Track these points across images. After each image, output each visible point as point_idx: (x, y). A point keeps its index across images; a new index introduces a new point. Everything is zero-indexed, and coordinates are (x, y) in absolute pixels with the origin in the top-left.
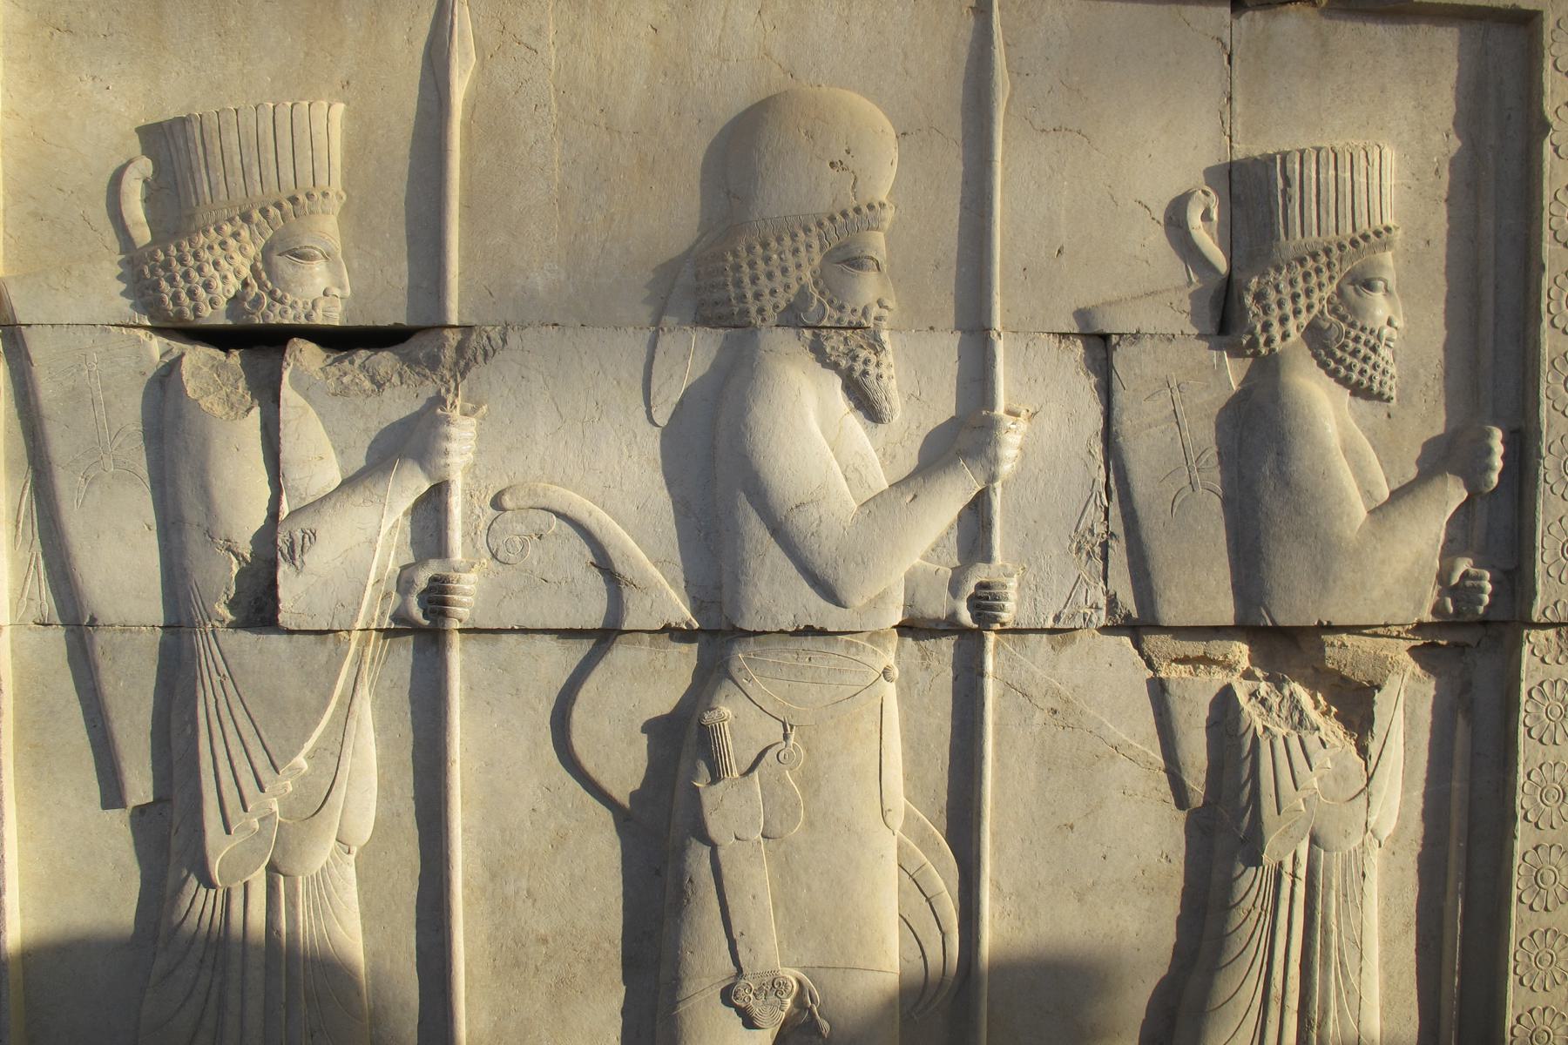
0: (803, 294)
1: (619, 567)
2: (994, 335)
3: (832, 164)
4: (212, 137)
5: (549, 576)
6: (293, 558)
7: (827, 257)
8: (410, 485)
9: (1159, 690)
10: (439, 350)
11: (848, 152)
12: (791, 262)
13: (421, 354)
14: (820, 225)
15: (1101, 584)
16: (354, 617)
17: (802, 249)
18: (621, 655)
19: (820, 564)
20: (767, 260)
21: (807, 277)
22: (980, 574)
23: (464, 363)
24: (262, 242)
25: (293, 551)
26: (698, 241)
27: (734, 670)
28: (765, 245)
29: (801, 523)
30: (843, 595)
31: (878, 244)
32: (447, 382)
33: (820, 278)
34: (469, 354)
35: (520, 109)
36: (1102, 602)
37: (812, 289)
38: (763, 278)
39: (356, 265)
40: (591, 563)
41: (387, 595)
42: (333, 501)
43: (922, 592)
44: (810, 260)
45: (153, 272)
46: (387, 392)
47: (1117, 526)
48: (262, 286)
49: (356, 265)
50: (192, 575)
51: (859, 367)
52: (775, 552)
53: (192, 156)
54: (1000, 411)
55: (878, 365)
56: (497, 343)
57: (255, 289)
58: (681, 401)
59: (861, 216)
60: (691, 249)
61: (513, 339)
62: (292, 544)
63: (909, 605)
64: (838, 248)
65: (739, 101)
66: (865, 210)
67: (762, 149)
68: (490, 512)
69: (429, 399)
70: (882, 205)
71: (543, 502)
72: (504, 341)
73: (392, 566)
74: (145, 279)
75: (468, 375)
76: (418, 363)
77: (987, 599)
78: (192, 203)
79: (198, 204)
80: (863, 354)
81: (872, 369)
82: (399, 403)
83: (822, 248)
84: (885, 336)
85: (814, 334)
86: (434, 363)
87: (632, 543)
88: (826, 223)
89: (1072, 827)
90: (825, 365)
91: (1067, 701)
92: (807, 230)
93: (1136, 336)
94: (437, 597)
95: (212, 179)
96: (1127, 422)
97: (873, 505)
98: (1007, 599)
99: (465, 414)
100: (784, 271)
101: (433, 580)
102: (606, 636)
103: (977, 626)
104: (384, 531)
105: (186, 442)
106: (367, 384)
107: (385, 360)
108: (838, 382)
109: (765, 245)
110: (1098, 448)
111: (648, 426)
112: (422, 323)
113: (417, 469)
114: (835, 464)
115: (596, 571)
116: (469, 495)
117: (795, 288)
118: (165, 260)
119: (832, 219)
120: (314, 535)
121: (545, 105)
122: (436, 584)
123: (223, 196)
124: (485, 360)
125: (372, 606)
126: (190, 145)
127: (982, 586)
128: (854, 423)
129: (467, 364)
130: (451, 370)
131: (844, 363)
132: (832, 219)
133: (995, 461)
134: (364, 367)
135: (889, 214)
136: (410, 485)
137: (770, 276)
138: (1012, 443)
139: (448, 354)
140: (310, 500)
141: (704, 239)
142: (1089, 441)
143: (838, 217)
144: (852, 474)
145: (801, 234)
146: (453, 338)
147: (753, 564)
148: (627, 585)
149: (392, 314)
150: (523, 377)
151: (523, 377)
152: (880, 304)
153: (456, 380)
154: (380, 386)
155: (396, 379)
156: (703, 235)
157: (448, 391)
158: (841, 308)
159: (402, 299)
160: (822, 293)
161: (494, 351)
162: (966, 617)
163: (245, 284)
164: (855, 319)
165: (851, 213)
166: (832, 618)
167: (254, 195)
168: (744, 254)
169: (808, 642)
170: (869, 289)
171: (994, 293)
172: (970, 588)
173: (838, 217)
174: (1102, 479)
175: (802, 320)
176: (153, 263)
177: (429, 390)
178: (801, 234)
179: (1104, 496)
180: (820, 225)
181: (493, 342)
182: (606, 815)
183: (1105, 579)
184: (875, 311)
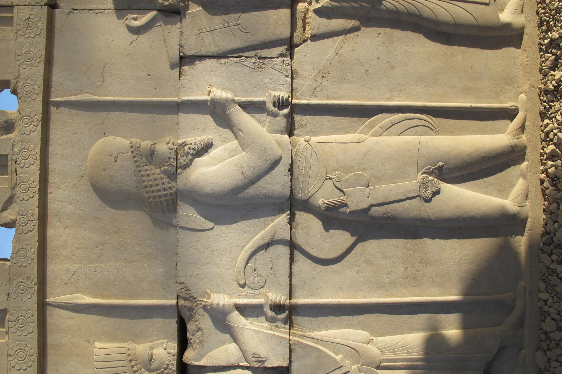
0: (164, 172)
1: (267, 241)
2: (180, 100)
3: (116, 161)
5: (270, 266)
7: (150, 163)
8: (236, 318)
9: (315, 38)
11: (111, 155)
12: (152, 177)
13: (188, 313)
14: (138, 166)
15: (274, 59)
16: (285, 339)
17: (147, 173)
18: (300, 240)
19: (265, 166)
20: (151, 186)
21: (158, 171)
22: (270, 106)
23: (191, 298)
26: (145, 211)
27: (305, 198)
28: (146, 187)
29: (250, 173)
30: (277, 158)
31: (146, 144)
32: (198, 304)
33: (158, 166)
34: (188, 296)
35: (96, 277)
36: (281, 59)
37: (162, 169)
38: (159, 187)
39: (155, 338)
40: (265, 251)
41: (277, 326)
43: (277, 128)
44: (152, 170)
46: (202, 326)
47: (252, 53)
49: (155, 338)
51: (191, 152)
52: (261, 183)
54: (208, 98)
55: (191, 144)
56: (183, 286)
58: (205, 218)
59: (135, 151)
60: (148, 214)
61: (182, 280)
63: (281, 132)
64: (147, 159)
65: (93, 196)
66: (133, 149)
67: (110, 188)
68: (246, 288)
69: (204, 311)
70: (131, 143)
71: (242, 269)
72: (183, 283)
73: (266, 324)
75: (195, 297)
76: (191, 315)
77: (279, 103)
80: (187, 150)
81: (192, 147)
82: (206, 322)
83: (147, 165)
84: (180, 142)
85: (179, 168)
86: (191, 309)
87: (258, 236)
88: (137, 164)
89: (367, 71)
90: (191, 164)
91: (319, 72)
92: (140, 171)
93: (181, 46)
94: (278, 308)
96: (213, 50)
97: (243, 146)
98: (279, 96)
99: (210, 298)
100: (155, 179)
101: (271, 309)
102: (292, 246)
103: (290, 107)
104: (253, 328)
106: (199, 333)
107: (190, 327)
108: (197, 159)
109: (146, 187)
110: (223, 61)
111: (214, 230)
112: (176, 313)
113: (230, 315)
114: (228, 160)
115: (268, 249)
116: (240, 296)
117: (162, 175)
119: (136, 161)
121: (95, 268)
122: (272, 308)
124: (190, 290)
125: (281, 332)
127: (274, 105)
128: (213, 153)
129: (191, 297)
130: (193, 303)
131: (190, 157)
132: (136, 161)
133: (227, 100)
134: (193, 334)
135: (135, 140)
136: (236, 318)
137: (157, 185)
138: (220, 94)
139: (188, 304)
141: (144, 209)
142: (220, 64)
143: (135, 159)
144: (232, 154)
145: (142, 173)
146: (182, 302)
147: (265, 191)
148: (273, 238)
149: (173, 325)
150: (196, 276)
151: (196, 276)
152: (168, 143)
153: (197, 301)
154: (199, 329)
155: (197, 323)
157: (201, 304)
158: (169, 158)
159: (167, 321)
160: (164, 165)
161: (186, 287)
162: (286, 111)
164: (174, 153)
165: (134, 154)
166: (286, 161)
168: (149, 195)
169: (295, 170)
170: (163, 148)
171: (164, 100)
172: (275, 110)
173: (135, 159)
174: (235, 59)
177: (201, 311)
178: (142, 173)
179: (241, 58)
180: (138, 166)
181: (183, 287)
182: (360, 245)
183: (272, 58)
184: (171, 145)
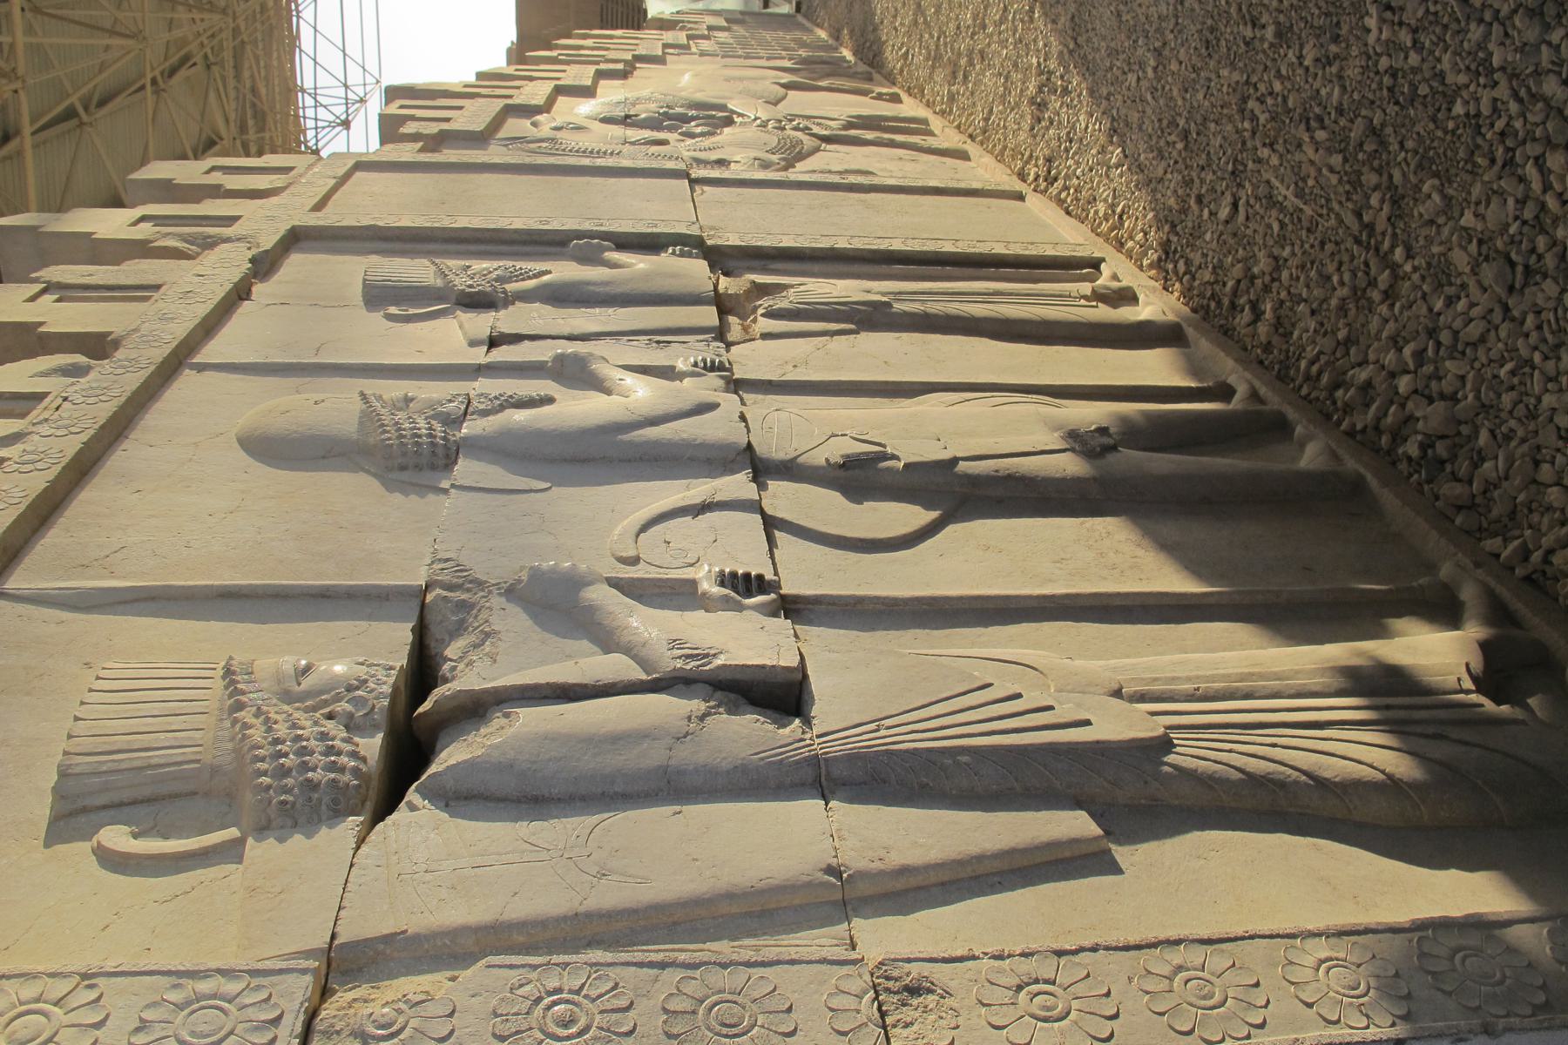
4: (105, 743)
6: (706, 656)
10: (451, 601)
24: (275, 701)
25: (698, 655)
26: (368, 472)
27: (789, 457)
34: (460, 581)
42: (631, 638)
45: (288, 791)
48: (338, 698)
50: (744, 759)
53: (124, 766)
57: (344, 706)
60: (375, 475)
62: (688, 656)
68: (642, 565)
74: (294, 804)
76: (463, 621)
78: (192, 769)
79: (198, 761)
85: (472, 414)
86: (465, 606)
95: (167, 744)
101: (722, 584)
105: (550, 760)
111: (550, 492)
112: (417, 613)
118: (272, 777)
120: (675, 641)
122: (726, 582)
123: (198, 735)
124: (466, 571)
126: (104, 768)
129: (471, 582)
130: (475, 594)
147: (685, 436)
156: (363, 470)
161: (458, 565)
163: (330, 717)
167: (207, 707)
175: (458, 418)
176: (271, 792)
182: (952, 530)
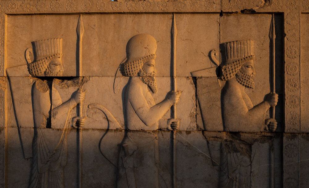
0: (140, 71)
1: (109, 118)
2: (174, 77)
3: (145, 48)
5: (97, 120)
7: (144, 64)
8: (73, 104)
11: (148, 45)
12: (138, 66)
14: (143, 58)
15: (195, 123)
17: (140, 63)
18: (109, 134)
19: (143, 118)
20: (134, 65)
21: (141, 68)
22: (172, 120)
23: (83, 82)
24: (49, 63)
28: (133, 62)
29: (140, 111)
30: (147, 124)
31: (153, 62)
32: (80, 86)
33: (143, 68)
34: (83, 81)
36: (196, 126)
37: (142, 70)
38: (133, 68)
41: (70, 123)
43: (162, 124)
44: (141, 65)
46: (70, 88)
47: (199, 112)
51: (150, 83)
52: (136, 116)
54: (176, 91)
55: (153, 83)
57: (48, 70)
59: (150, 57)
61: (91, 79)
63: (159, 126)
64: (146, 63)
66: (151, 56)
70: (154, 55)
72: (89, 79)
73: (71, 117)
75: (83, 85)
77: (173, 125)
80: (151, 81)
81: (152, 84)
82: (72, 90)
83: (143, 63)
84: (154, 78)
87: (111, 114)
88: (144, 58)
89: (191, 168)
90: (144, 82)
91: (189, 144)
92: (141, 60)
93: (201, 77)
94: (78, 123)
96: (199, 93)
97: (152, 108)
98: (177, 125)
99: (83, 92)
100: (137, 67)
102: (108, 130)
104: (69, 112)
106: (66, 86)
107: (70, 82)
108: (147, 86)
109: (133, 62)
110: (194, 98)
113: (75, 101)
114: (146, 101)
116: (83, 105)
117: (139, 70)
119: (145, 57)
125: (67, 124)
127: (172, 123)
128: (149, 93)
131: (147, 83)
132: (145, 57)
133: (175, 100)
135: (155, 56)
136: (73, 104)
137: (134, 68)
138: (177, 98)
139: (80, 81)
140: (57, 106)
142: (192, 96)
143: (146, 57)
144: (149, 102)
145: (140, 60)
146: (81, 79)
152: (154, 72)
155: (71, 85)
158: (147, 73)
160: (143, 71)
162: (170, 128)
163: (46, 70)
164: (149, 75)
165: (148, 56)
166: (146, 128)
168: (130, 64)
170: (151, 70)
171: (174, 70)
172: (171, 123)
173: (146, 57)
174: (195, 104)
177: (77, 88)
178: (140, 60)
179: (196, 106)
180: (143, 58)
183: (196, 122)
184: (153, 73)
